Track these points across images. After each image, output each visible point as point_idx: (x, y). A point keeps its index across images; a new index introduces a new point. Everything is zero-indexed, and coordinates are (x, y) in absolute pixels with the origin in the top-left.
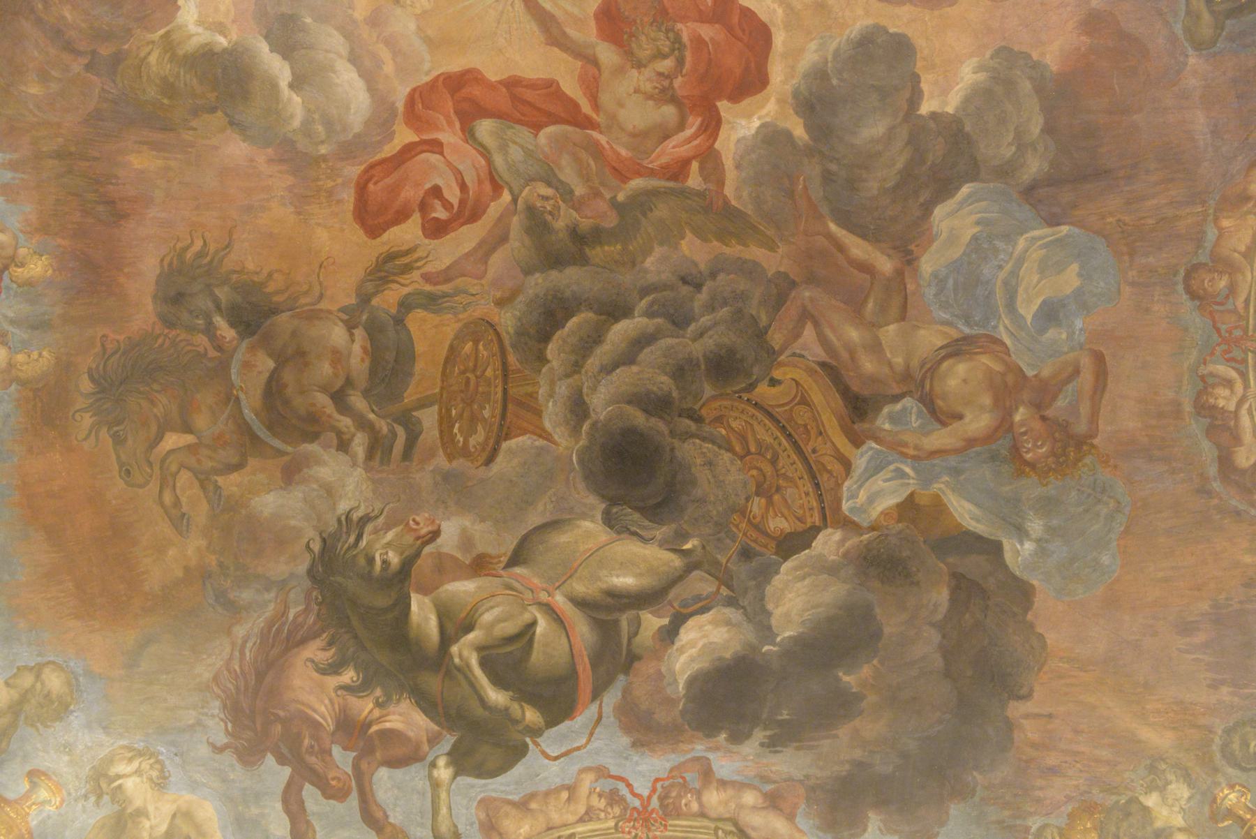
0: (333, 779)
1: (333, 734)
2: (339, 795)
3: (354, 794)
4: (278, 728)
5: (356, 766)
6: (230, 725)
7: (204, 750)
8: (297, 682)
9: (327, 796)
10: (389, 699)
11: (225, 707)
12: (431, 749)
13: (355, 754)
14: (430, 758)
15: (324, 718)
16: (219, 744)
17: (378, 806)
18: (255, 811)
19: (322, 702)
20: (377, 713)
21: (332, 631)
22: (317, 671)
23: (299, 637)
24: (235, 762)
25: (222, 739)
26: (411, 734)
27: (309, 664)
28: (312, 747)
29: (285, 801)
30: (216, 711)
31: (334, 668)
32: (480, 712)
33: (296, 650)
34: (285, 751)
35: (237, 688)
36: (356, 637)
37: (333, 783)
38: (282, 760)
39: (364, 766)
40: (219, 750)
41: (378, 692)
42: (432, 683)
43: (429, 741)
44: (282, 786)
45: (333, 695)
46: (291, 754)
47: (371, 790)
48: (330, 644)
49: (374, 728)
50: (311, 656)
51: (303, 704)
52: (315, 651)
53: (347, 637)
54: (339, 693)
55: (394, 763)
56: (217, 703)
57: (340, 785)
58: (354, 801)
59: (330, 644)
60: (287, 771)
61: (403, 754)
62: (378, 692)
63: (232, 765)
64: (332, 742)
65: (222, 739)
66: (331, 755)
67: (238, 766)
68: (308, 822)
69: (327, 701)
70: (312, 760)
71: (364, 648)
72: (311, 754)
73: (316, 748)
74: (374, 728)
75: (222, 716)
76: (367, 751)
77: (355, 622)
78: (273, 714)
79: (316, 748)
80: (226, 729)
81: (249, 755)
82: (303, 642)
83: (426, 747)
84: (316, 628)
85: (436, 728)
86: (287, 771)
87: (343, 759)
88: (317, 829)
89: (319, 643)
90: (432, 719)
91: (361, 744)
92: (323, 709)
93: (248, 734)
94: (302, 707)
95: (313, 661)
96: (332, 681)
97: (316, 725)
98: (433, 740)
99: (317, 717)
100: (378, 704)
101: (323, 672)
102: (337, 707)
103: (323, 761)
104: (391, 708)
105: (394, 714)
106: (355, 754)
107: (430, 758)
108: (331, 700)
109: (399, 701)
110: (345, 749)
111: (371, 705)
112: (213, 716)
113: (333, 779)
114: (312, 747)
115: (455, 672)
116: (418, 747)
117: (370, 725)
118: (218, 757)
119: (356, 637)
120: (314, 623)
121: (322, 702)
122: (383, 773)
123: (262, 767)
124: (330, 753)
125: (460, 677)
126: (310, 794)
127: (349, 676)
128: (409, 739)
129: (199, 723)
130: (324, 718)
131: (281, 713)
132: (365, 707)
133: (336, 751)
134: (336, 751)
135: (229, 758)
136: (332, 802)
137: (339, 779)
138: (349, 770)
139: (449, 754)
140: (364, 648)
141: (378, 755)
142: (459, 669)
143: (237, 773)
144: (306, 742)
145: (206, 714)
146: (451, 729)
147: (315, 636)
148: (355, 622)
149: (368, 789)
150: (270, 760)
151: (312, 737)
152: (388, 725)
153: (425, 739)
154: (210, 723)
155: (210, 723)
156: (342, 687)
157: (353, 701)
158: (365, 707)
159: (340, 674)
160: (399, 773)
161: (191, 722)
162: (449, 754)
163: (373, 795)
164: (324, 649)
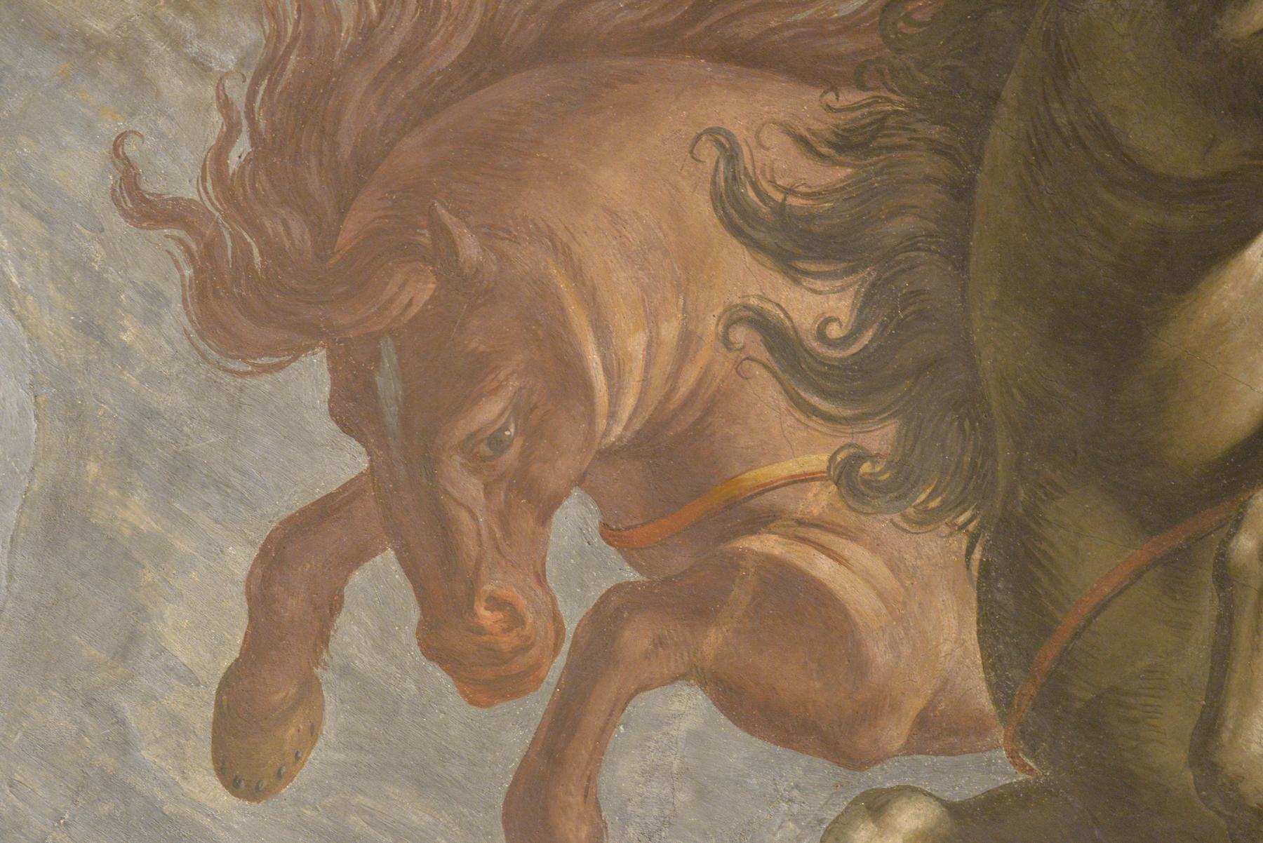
0: (496, 603)
1: (608, 455)
2: (487, 675)
3: (535, 706)
4: (421, 291)
5: (607, 618)
6: (242, 148)
7: (80, 169)
8: (614, 182)
9: (434, 645)
10: (902, 482)
11: (270, 66)
12: (908, 749)
13: (631, 575)
14: (879, 777)
15: (615, 376)
16: (152, 186)
17: (589, 793)
18: (137, 514)
19: (653, 319)
20: (818, 500)
21: (897, 103)
22: (717, 200)
23: (747, 29)
24: (173, 292)
25: (178, 176)
26: (880, 654)
27: (709, 153)
28: (498, 443)
29: (275, 557)
30: (230, 59)
31: (795, 242)
32: (1169, 756)
33: (704, 67)
34: (388, 384)
35: (367, 32)
36: (961, 191)
37: (486, 616)
38: (353, 408)
39: (636, 637)
40: (148, 210)
41: (881, 437)
42: (1096, 551)
43: (923, 722)
44: (295, 500)
45: (711, 325)
46: (405, 413)
47: (604, 733)
48: (848, 143)
49: (769, 544)
50: (740, 131)
51: (576, 273)
52: (770, 128)
53: (925, 163)
54: (740, 335)
55: (746, 703)
56: (250, 34)
57: (507, 642)
58: (516, 727)
59: (848, 143)
60: (347, 461)
61: (798, 692)
62: (881, 437)
63: (154, 297)
64: (581, 481)
65: (178, 176)
66: (544, 517)
67: (177, 315)
68: (309, 689)
69: (670, 331)
70: (466, 488)
71: (959, 256)
72: (476, 463)
73: (510, 457)
74: (769, 544)
75: (238, 95)
76: (691, 601)
77: (1002, 140)
78: (439, 229)
79: (510, 457)
80: (220, 153)
81: (245, 307)
82: (752, 58)
83: (896, 733)
84: (846, 45)
85: (983, 700)
86: (347, 461)
87: (577, 559)
88: (329, 729)
89: (809, 107)
90: (992, 662)
91: (680, 560)
92: (636, 345)
93: (297, 234)
94: (563, 285)
95: (731, 154)
96: (746, 277)
97: (567, 381)
98: (939, 730)
99: (593, 358)
100: (845, 475)
101: (738, 218)
102: (690, 376)
103: (504, 518)
104: (881, 524)
105: (875, 547)
106: (631, 575)
107: (879, 777)
108: (687, 340)
109: (927, 519)
110: (610, 533)
111: (817, 461)
112: (200, 67)
113: (496, 603)
114: (498, 443)
115: (1207, 576)
116: (871, 711)
117: (761, 521)
118: (118, 225)
119: (961, 191)
120: (849, 26)
121: (653, 319)
122: (688, 707)
123: (265, 383)
124: (546, 509)
125: (1208, 604)
126: (379, 590)
127: (821, 306)
128: (858, 665)
129: (127, 52)
130: (615, 376)
131: (470, 248)
132: (790, 448)
133: (574, 519)
134: (574, 519)
135: (159, 262)
136: (439, 676)
137: (515, 619)
138: (573, 616)
139: (955, 810)
140: (959, 256)
141: (713, 640)
142: (1225, 576)
143: (157, 337)
144: (489, 411)
145: (176, 42)
146: (1027, 739)
147: (812, 71)
148: (1002, 140)
149: (593, 721)
150: (311, 378)
151: (521, 409)
152: (823, 568)
153: (914, 705)
154: (174, 85)
155: (174, 85)
156: (761, 323)
157: (766, 395)
158: (790, 448)
159: (794, 275)
160: (738, 748)
161: (98, 26)
162: (955, 810)
163: (598, 753)
164: (804, 143)
